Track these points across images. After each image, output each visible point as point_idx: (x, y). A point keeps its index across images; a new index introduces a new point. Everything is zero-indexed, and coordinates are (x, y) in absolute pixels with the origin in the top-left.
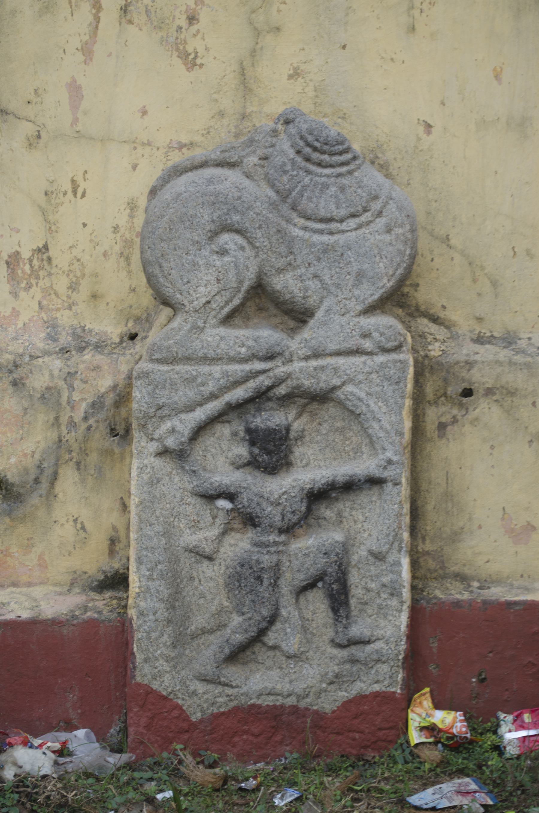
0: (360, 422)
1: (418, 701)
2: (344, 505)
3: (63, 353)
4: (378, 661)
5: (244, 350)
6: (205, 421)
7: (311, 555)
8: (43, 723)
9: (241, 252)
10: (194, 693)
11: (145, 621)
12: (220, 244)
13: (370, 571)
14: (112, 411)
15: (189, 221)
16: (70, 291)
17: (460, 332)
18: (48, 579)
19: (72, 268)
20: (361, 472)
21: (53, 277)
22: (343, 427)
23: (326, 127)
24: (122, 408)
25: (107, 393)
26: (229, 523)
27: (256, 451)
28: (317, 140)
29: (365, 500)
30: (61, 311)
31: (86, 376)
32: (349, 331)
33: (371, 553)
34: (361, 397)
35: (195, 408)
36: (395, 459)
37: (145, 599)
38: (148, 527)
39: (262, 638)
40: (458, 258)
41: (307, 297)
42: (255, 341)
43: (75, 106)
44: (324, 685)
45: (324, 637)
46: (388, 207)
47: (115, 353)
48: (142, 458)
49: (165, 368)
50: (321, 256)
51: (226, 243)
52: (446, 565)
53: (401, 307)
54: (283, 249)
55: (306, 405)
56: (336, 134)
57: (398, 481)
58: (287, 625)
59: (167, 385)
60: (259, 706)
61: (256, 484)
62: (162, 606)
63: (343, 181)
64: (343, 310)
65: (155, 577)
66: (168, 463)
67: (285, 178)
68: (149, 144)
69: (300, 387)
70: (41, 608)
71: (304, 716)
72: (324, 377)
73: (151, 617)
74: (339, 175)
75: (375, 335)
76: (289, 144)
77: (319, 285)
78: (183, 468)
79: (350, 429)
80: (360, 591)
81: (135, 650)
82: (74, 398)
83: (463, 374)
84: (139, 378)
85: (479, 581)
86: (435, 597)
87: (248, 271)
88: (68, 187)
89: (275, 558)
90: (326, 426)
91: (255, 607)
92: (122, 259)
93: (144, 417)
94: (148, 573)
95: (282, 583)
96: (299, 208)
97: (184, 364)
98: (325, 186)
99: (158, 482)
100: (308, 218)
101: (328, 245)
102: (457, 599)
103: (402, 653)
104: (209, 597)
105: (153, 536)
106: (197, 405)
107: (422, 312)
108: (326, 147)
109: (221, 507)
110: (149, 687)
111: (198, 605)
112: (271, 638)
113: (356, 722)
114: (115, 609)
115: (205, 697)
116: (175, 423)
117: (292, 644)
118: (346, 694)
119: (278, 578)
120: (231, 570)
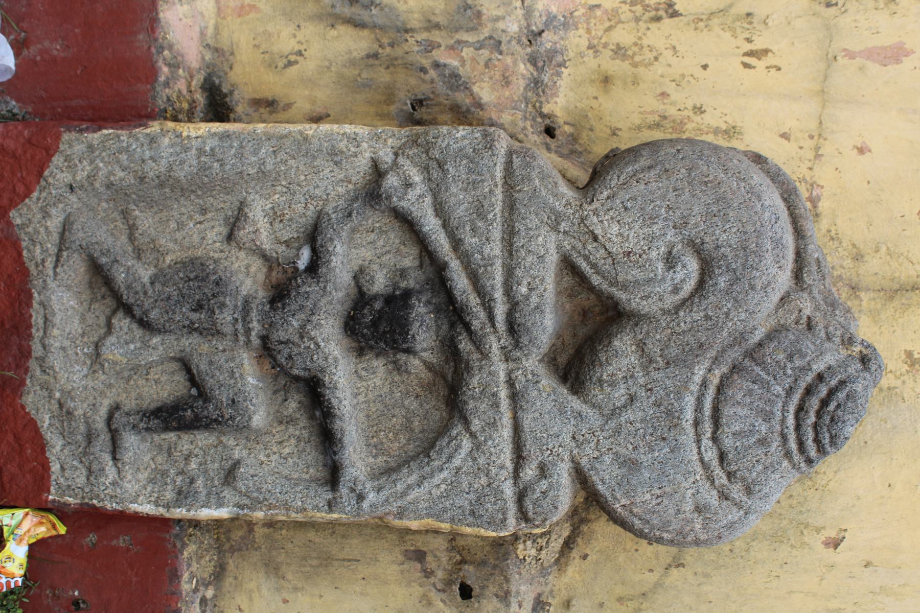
0: (418, 455)
1: (44, 521)
2: (302, 428)
3: (528, 36)
4: (90, 471)
5: (524, 290)
6: (421, 231)
7: (232, 381)
8: (24, 10)
9: (670, 289)
10: (46, 215)
11: (143, 145)
12: (683, 258)
13: (213, 462)
14: (446, 102)
15: (719, 211)
16: (614, 47)
17: (550, 577)
18: (224, 18)
19: (646, 50)
20: (346, 455)
21: (633, 24)
22: (412, 430)
23: (858, 420)
24: (450, 116)
25: (472, 95)
26: (279, 265)
27: (378, 305)
28: (839, 406)
29: (310, 458)
30: (587, 36)
31: (495, 66)
32: (550, 446)
33: (237, 464)
34: (454, 461)
35: (440, 218)
36: (365, 505)
37: (172, 146)
38: (271, 149)
39: (121, 310)
40: (652, 578)
41: (601, 386)
42: (537, 308)
43: (871, 54)
44: (58, 395)
45: (124, 395)
46: (735, 509)
47: (527, 106)
48: (368, 141)
49: (499, 173)
50: (662, 408)
51: (684, 266)
52: (236, 554)
53: (586, 499)
54: (673, 351)
55: (444, 377)
56: (847, 435)
57: (334, 508)
58: (138, 345)
59: (473, 176)
60: (29, 305)
61: (331, 304)
62: (163, 170)
63: (775, 444)
64: (582, 438)
65: (203, 159)
66: (364, 178)
67: (781, 356)
68: (818, 156)
69: (468, 372)
70: (178, 6)
71: (18, 366)
72: (483, 407)
73: (148, 154)
74: (784, 438)
75: (544, 485)
76: (833, 363)
77: (618, 404)
78: (356, 199)
79: (409, 440)
80: (186, 447)
81: (105, 132)
82: (465, 49)
83: (491, 588)
84: (485, 135)
85: (215, 596)
86: (184, 545)
87: (641, 298)
88: (758, 45)
89: (228, 329)
90: (415, 405)
91: (162, 300)
92: (657, 118)
93: (428, 143)
94: (208, 148)
95: (195, 339)
96: (736, 376)
97: (504, 202)
98: (768, 417)
99: (336, 163)
100: (720, 389)
101: (679, 418)
102: (182, 576)
103: (101, 504)
104: (178, 236)
105: (259, 156)
106: (445, 221)
107: (579, 527)
108: (827, 418)
109: (300, 253)
110: (56, 151)
111: (168, 220)
112: (122, 323)
113: (10, 438)
114: (172, 105)
115: (42, 230)
116: (418, 188)
117: (113, 351)
118: (46, 425)
119: (201, 334)
120: (211, 267)
